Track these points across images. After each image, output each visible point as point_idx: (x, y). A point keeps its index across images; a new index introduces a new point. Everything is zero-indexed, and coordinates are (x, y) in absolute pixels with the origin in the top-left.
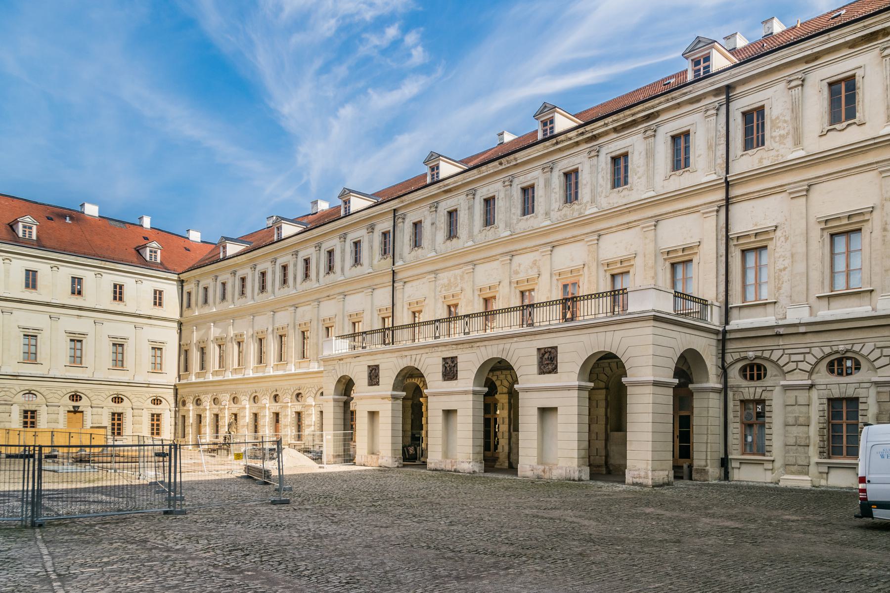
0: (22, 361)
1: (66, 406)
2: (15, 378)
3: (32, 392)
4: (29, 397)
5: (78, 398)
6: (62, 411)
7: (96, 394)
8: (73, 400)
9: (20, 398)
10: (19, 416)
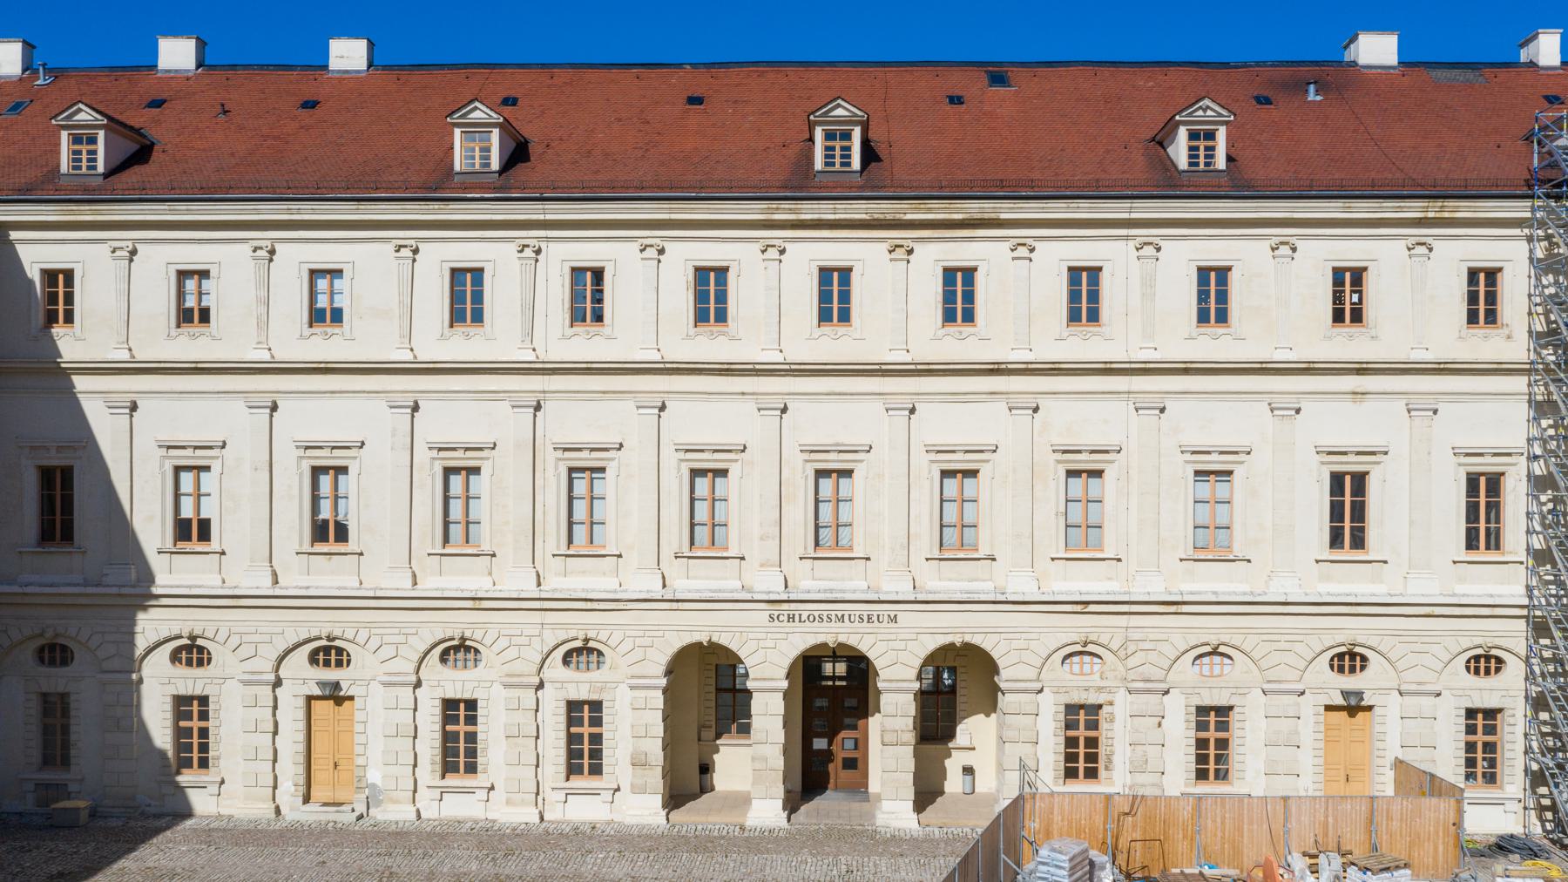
0: (1191, 553)
1: (1319, 690)
2: (1173, 609)
3: (1222, 649)
4: (1212, 664)
5: (1358, 663)
6: (1310, 707)
7: (1418, 647)
8: (1341, 670)
9: (1186, 671)
10: (1184, 725)
